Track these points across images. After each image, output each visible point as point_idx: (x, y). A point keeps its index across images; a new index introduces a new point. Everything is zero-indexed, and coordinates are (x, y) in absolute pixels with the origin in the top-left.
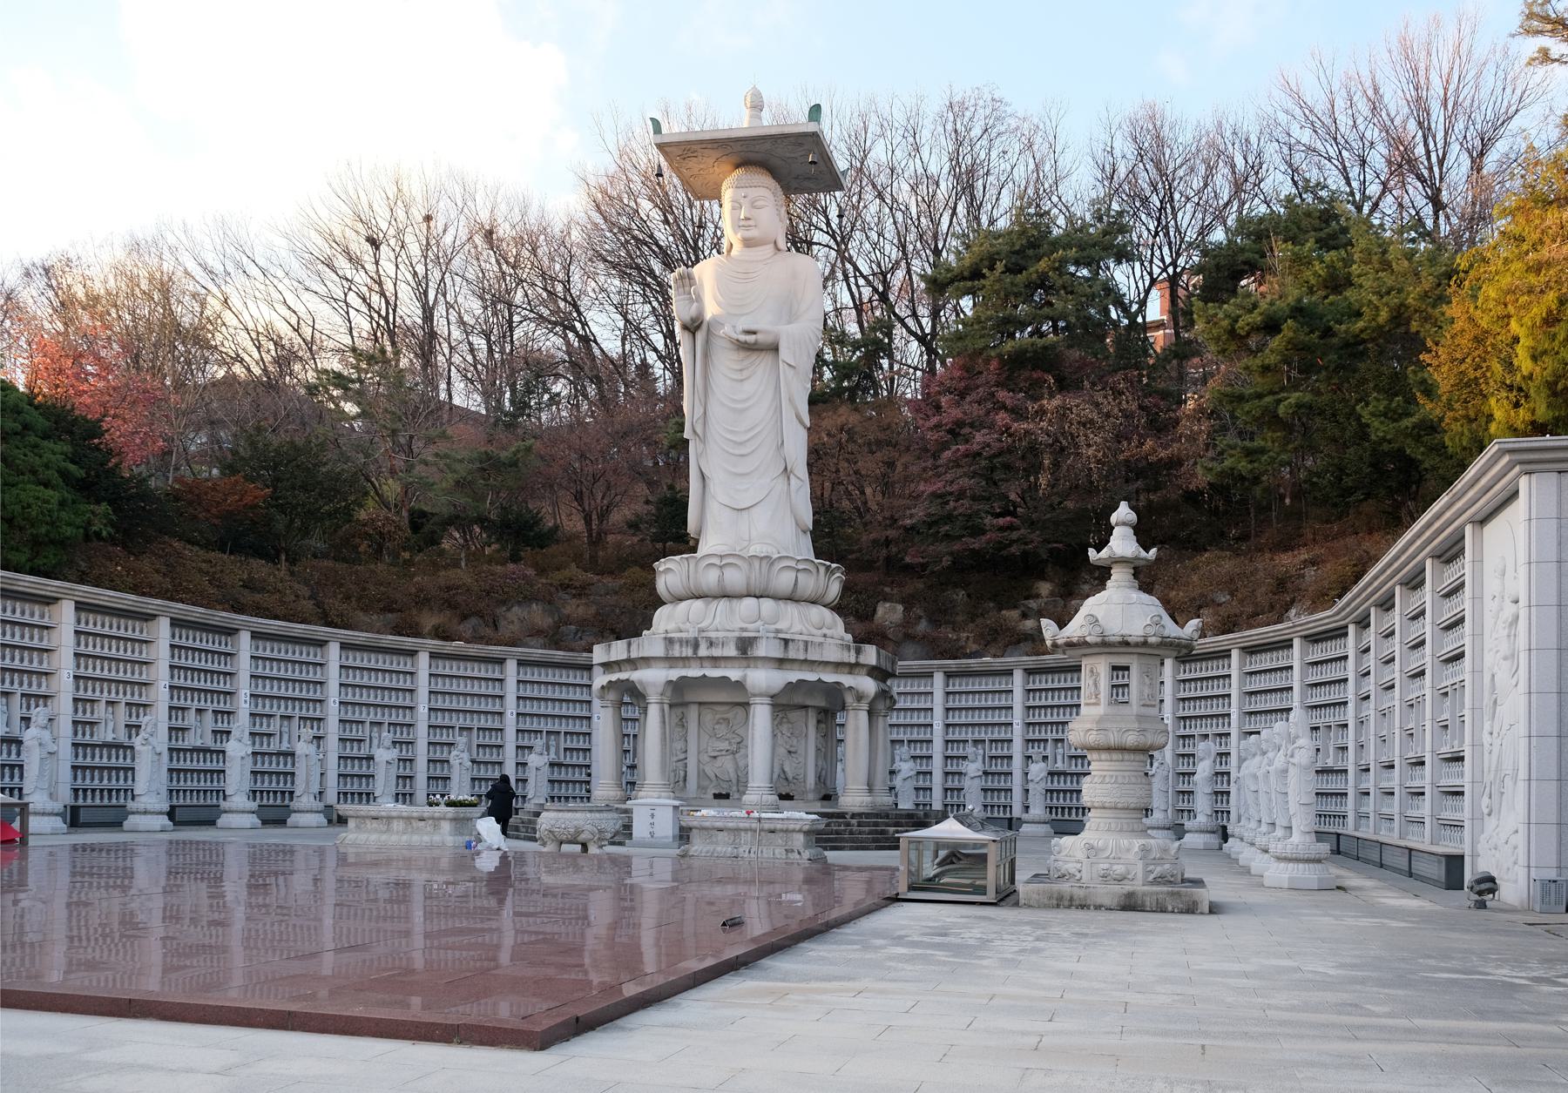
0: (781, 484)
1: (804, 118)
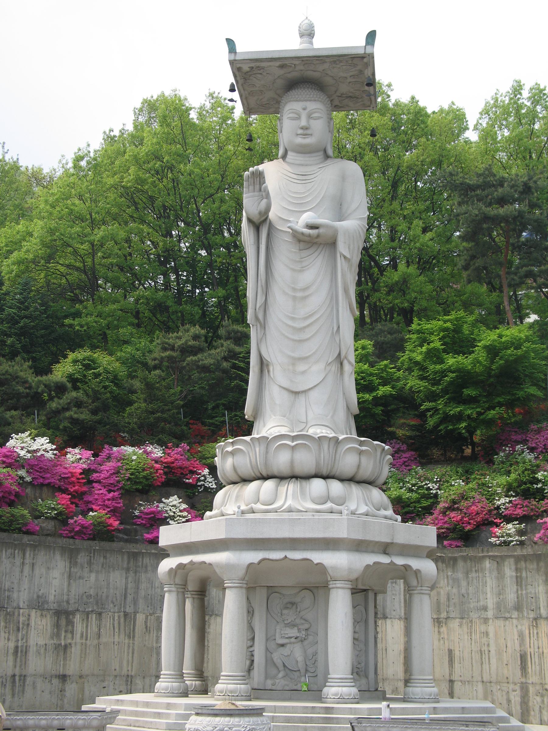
0: (334, 368)
1: (363, 43)
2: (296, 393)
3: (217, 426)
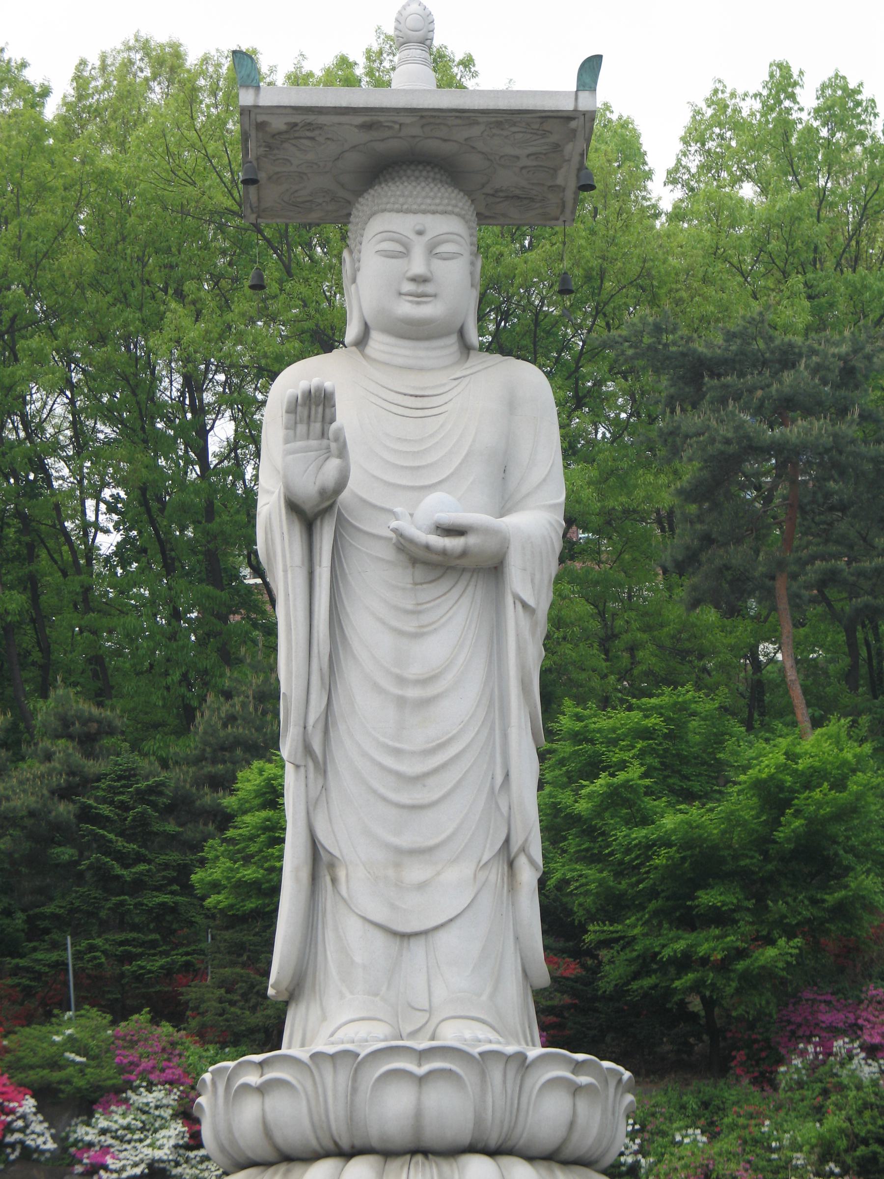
0: (496, 874)
2: (405, 937)
3: (38, 976)
